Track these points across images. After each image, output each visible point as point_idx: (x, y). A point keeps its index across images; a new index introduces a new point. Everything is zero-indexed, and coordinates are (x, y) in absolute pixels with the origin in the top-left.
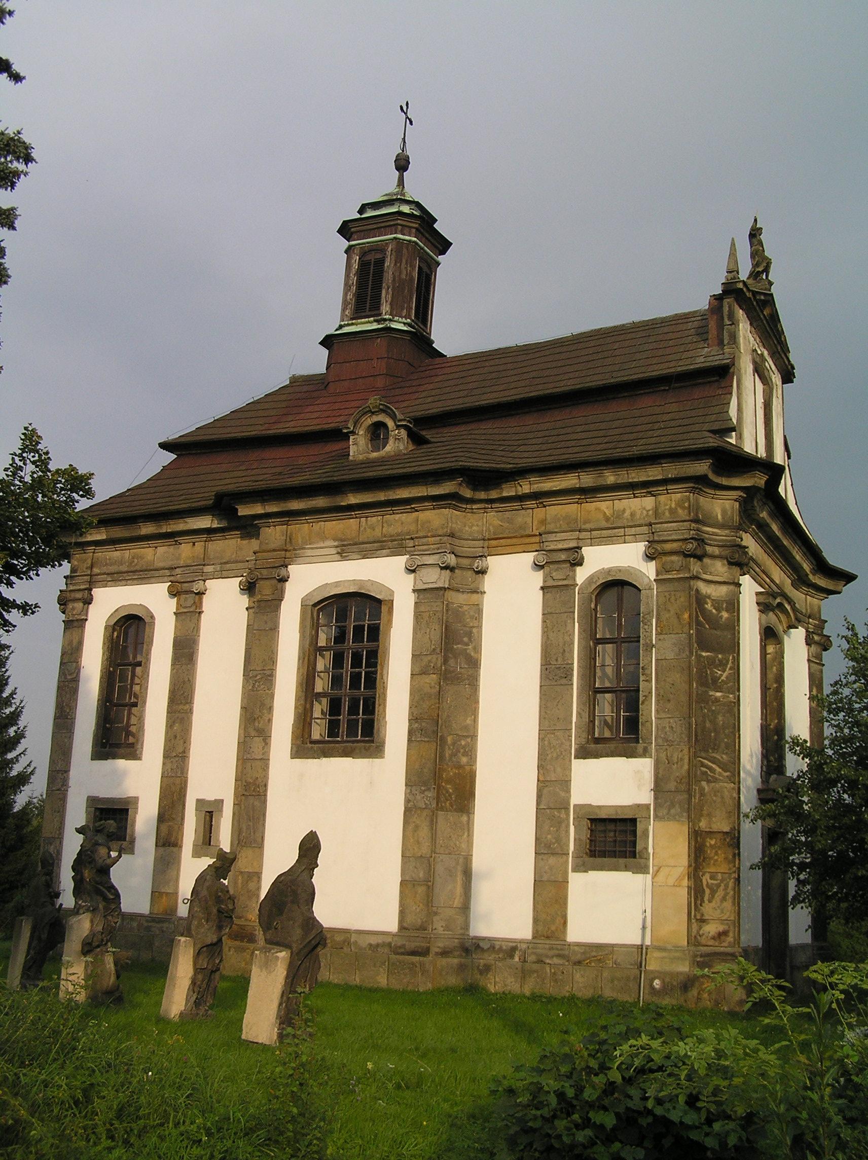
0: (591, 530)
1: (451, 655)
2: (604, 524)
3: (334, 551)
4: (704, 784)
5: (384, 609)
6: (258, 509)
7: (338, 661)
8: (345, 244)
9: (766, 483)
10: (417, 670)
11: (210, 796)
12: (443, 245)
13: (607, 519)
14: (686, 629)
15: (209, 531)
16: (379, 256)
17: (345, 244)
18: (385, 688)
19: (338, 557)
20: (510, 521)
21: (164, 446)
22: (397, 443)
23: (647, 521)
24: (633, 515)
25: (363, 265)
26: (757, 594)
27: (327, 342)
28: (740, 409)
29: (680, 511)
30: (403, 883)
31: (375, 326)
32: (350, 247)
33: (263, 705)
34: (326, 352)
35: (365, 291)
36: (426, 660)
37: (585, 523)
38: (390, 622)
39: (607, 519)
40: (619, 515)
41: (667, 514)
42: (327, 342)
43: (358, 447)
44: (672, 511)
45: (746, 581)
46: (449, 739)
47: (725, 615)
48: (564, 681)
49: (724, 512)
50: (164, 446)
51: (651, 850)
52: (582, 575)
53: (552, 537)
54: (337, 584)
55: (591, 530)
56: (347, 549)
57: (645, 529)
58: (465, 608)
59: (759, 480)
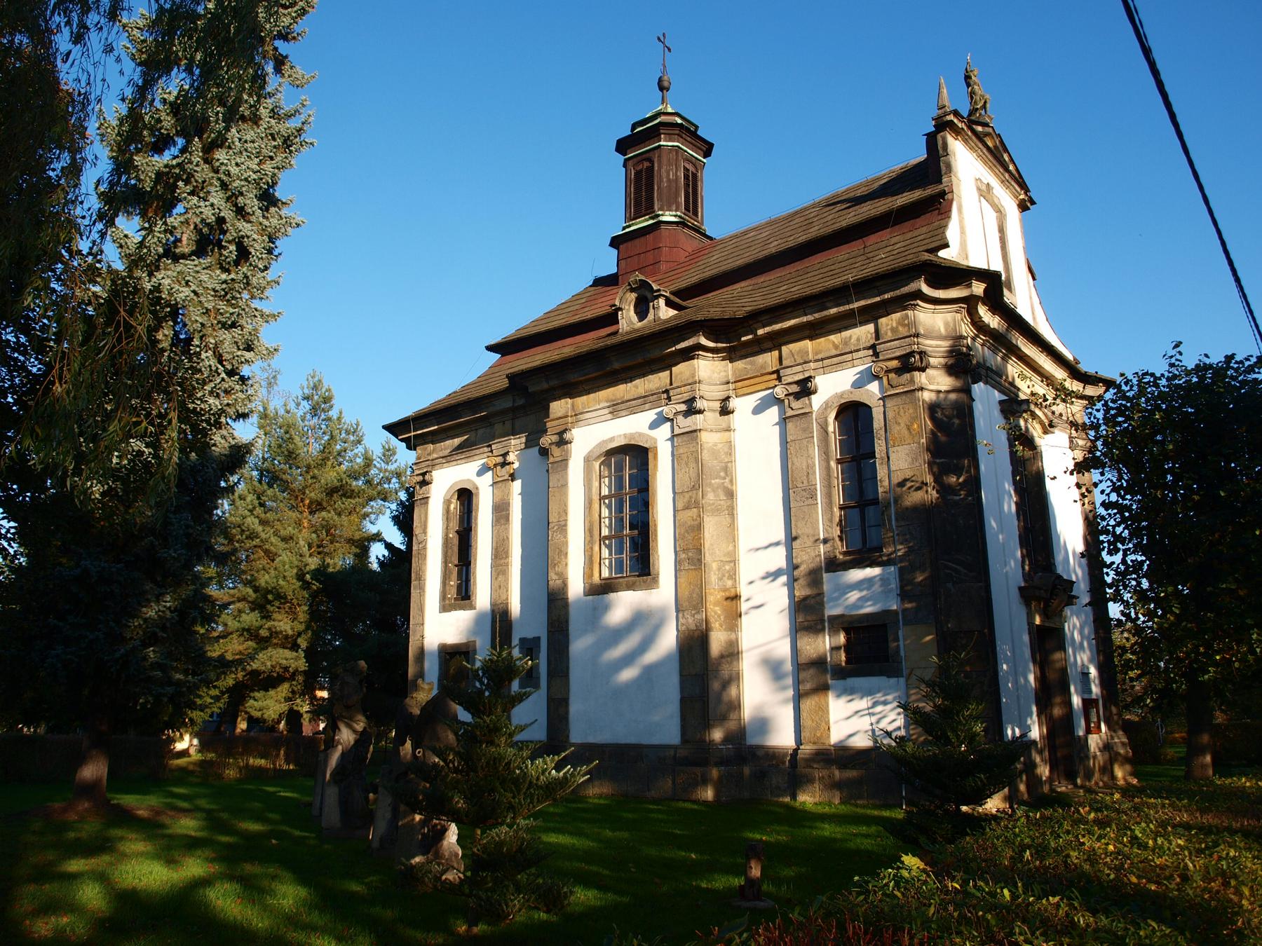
0: (822, 360)
1: (707, 489)
2: (834, 352)
3: (607, 411)
4: (950, 585)
5: (650, 455)
6: (545, 386)
7: (620, 509)
8: (622, 158)
9: (985, 290)
10: (680, 505)
11: (530, 635)
12: (708, 149)
13: (836, 347)
14: (916, 439)
15: (514, 410)
16: (646, 164)
17: (622, 158)
18: (656, 525)
19: (610, 416)
20: (752, 363)
21: (490, 348)
22: (666, 313)
23: (869, 344)
24: (858, 340)
25: (638, 174)
26: (1001, 402)
27: (616, 242)
28: (963, 232)
29: (900, 328)
30: (683, 701)
31: (651, 222)
32: (626, 160)
33: (561, 551)
34: (615, 252)
35: (641, 195)
36: (687, 496)
37: (817, 354)
38: (656, 466)
39: (836, 347)
40: (846, 342)
41: (889, 333)
42: (616, 242)
43: (629, 321)
44: (894, 330)
45: (979, 389)
46: (714, 566)
47: (957, 421)
48: (810, 501)
49: (946, 324)
50: (490, 348)
51: (902, 653)
52: (817, 401)
53: (788, 371)
54: (612, 439)
55: (822, 360)
56: (616, 409)
57: (871, 352)
58: (720, 446)
59: (978, 288)
